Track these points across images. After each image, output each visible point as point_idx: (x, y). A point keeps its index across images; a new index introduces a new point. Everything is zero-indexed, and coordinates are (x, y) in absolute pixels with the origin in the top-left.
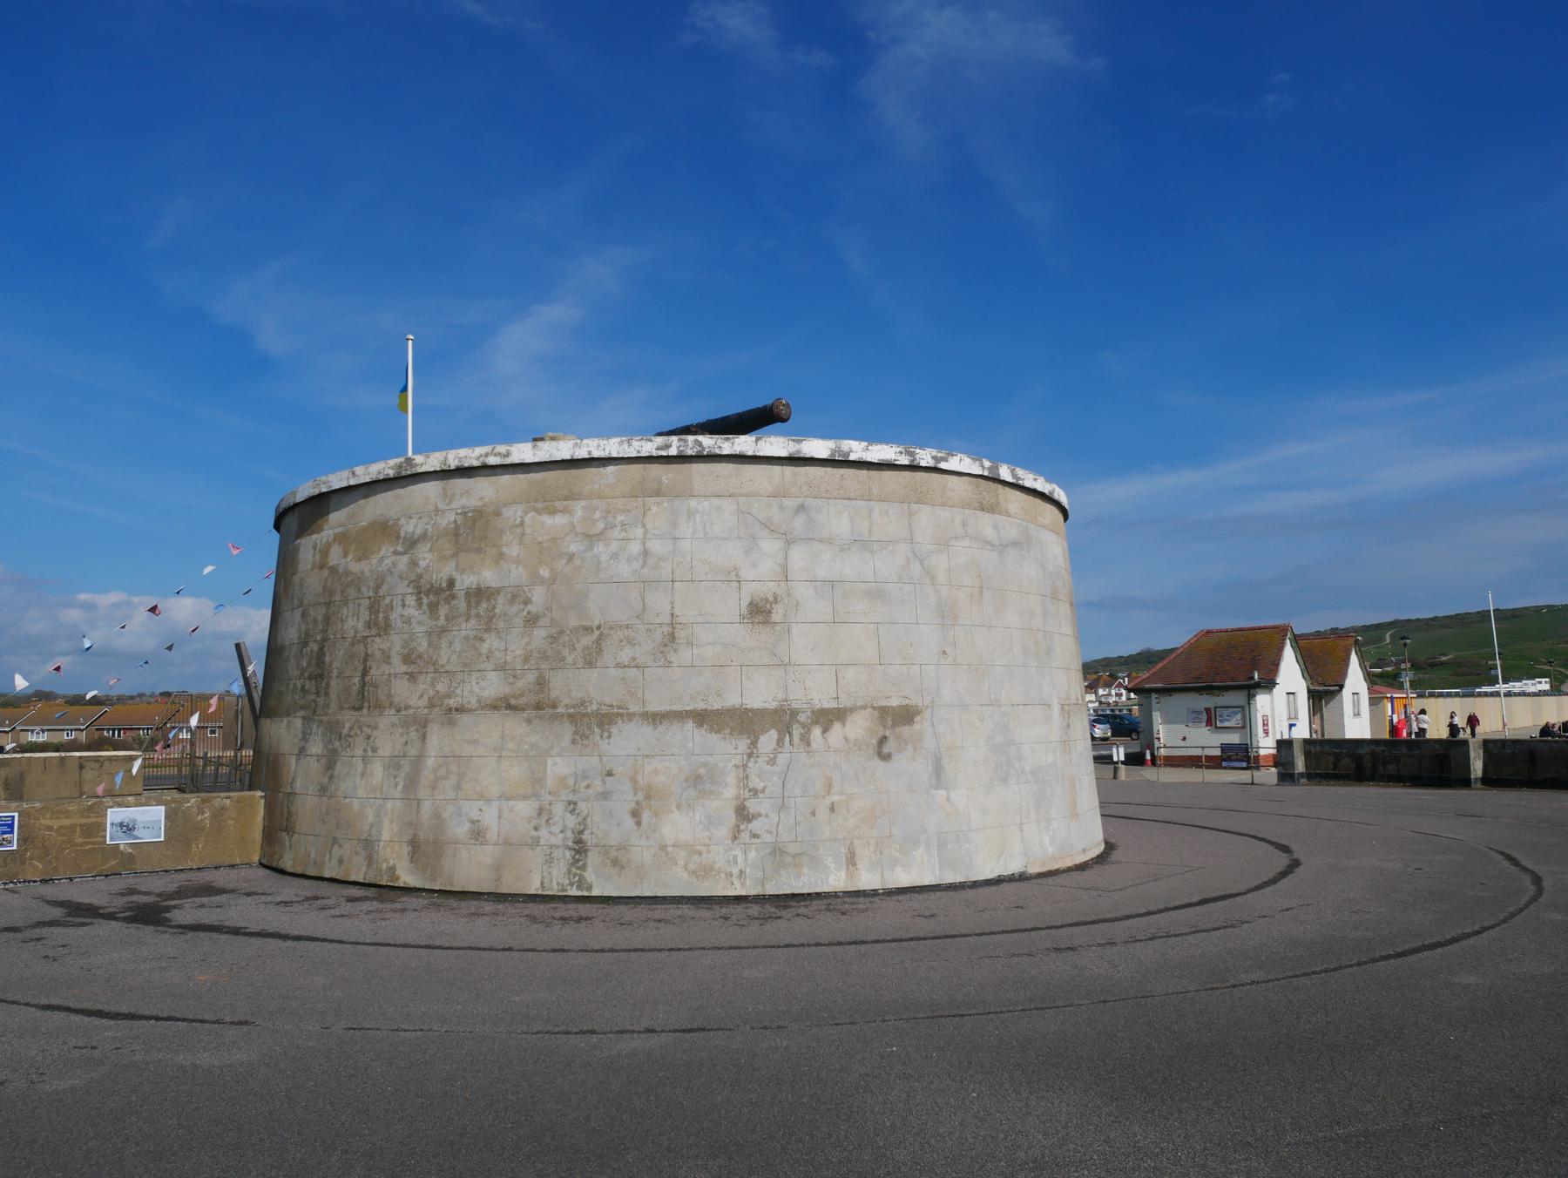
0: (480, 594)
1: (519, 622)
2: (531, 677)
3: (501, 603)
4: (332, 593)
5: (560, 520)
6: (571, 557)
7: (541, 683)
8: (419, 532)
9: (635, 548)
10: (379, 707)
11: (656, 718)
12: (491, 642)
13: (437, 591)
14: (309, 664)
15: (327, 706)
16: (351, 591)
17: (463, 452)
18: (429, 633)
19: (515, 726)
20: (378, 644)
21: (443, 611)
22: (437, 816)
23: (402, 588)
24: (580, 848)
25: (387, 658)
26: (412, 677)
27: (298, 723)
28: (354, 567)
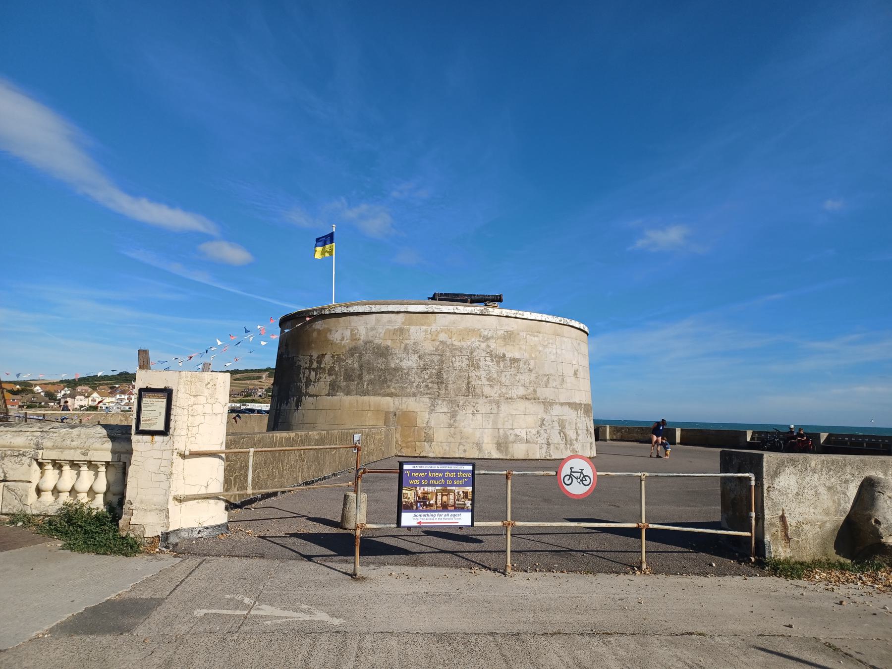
0: (514, 360)
1: (527, 371)
2: (532, 389)
3: (521, 364)
4: (443, 351)
5: (536, 339)
6: (540, 352)
7: (535, 391)
8: (489, 335)
9: (554, 351)
10: (477, 395)
11: (562, 404)
12: (519, 377)
13: (500, 357)
14: (430, 377)
15: (447, 394)
16: (457, 353)
17: (508, 311)
18: (497, 372)
19: (528, 404)
20: (474, 374)
21: (502, 364)
22: (505, 434)
23: (484, 354)
24: (548, 444)
25: (480, 379)
26: (491, 386)
27: (426, 399)
28: (456, 343)
